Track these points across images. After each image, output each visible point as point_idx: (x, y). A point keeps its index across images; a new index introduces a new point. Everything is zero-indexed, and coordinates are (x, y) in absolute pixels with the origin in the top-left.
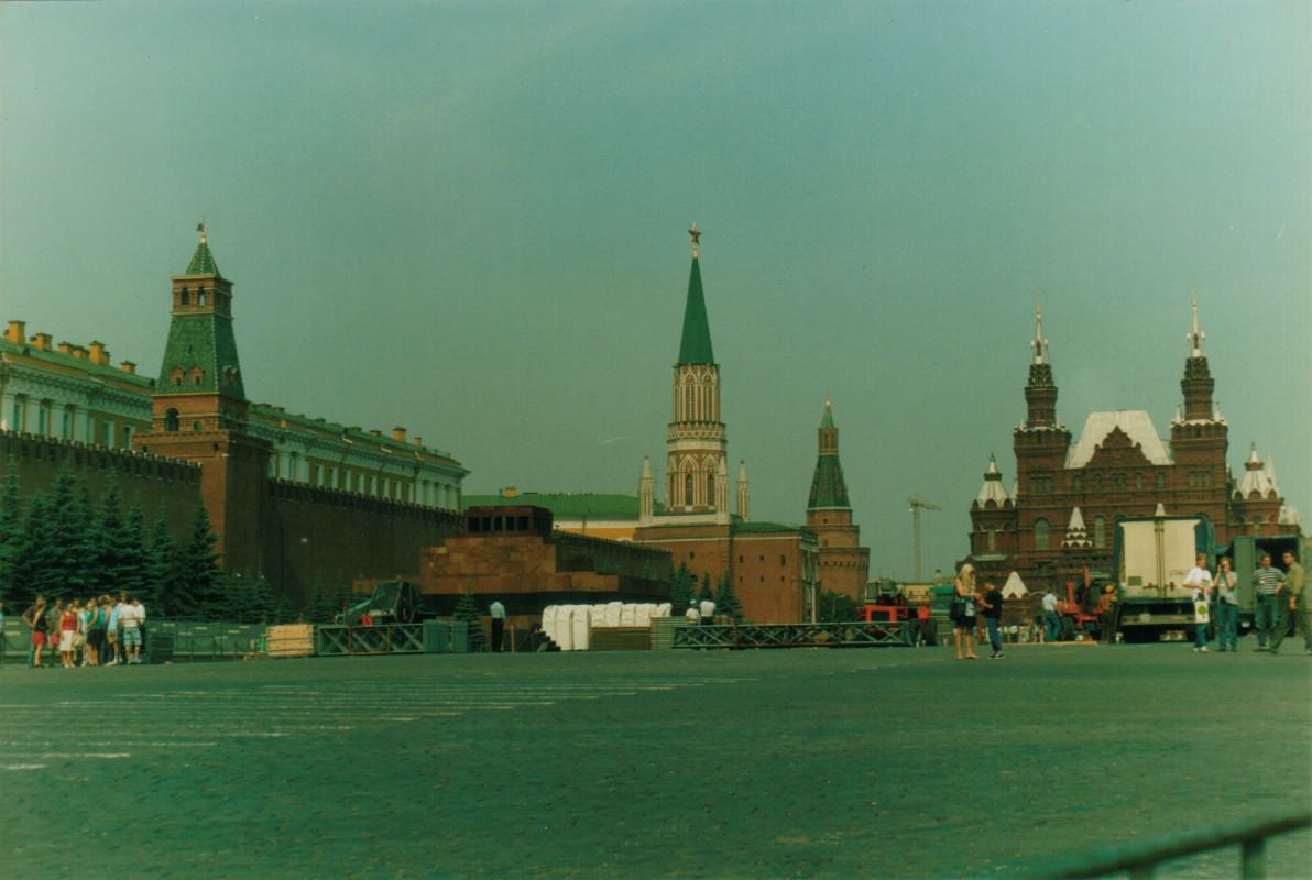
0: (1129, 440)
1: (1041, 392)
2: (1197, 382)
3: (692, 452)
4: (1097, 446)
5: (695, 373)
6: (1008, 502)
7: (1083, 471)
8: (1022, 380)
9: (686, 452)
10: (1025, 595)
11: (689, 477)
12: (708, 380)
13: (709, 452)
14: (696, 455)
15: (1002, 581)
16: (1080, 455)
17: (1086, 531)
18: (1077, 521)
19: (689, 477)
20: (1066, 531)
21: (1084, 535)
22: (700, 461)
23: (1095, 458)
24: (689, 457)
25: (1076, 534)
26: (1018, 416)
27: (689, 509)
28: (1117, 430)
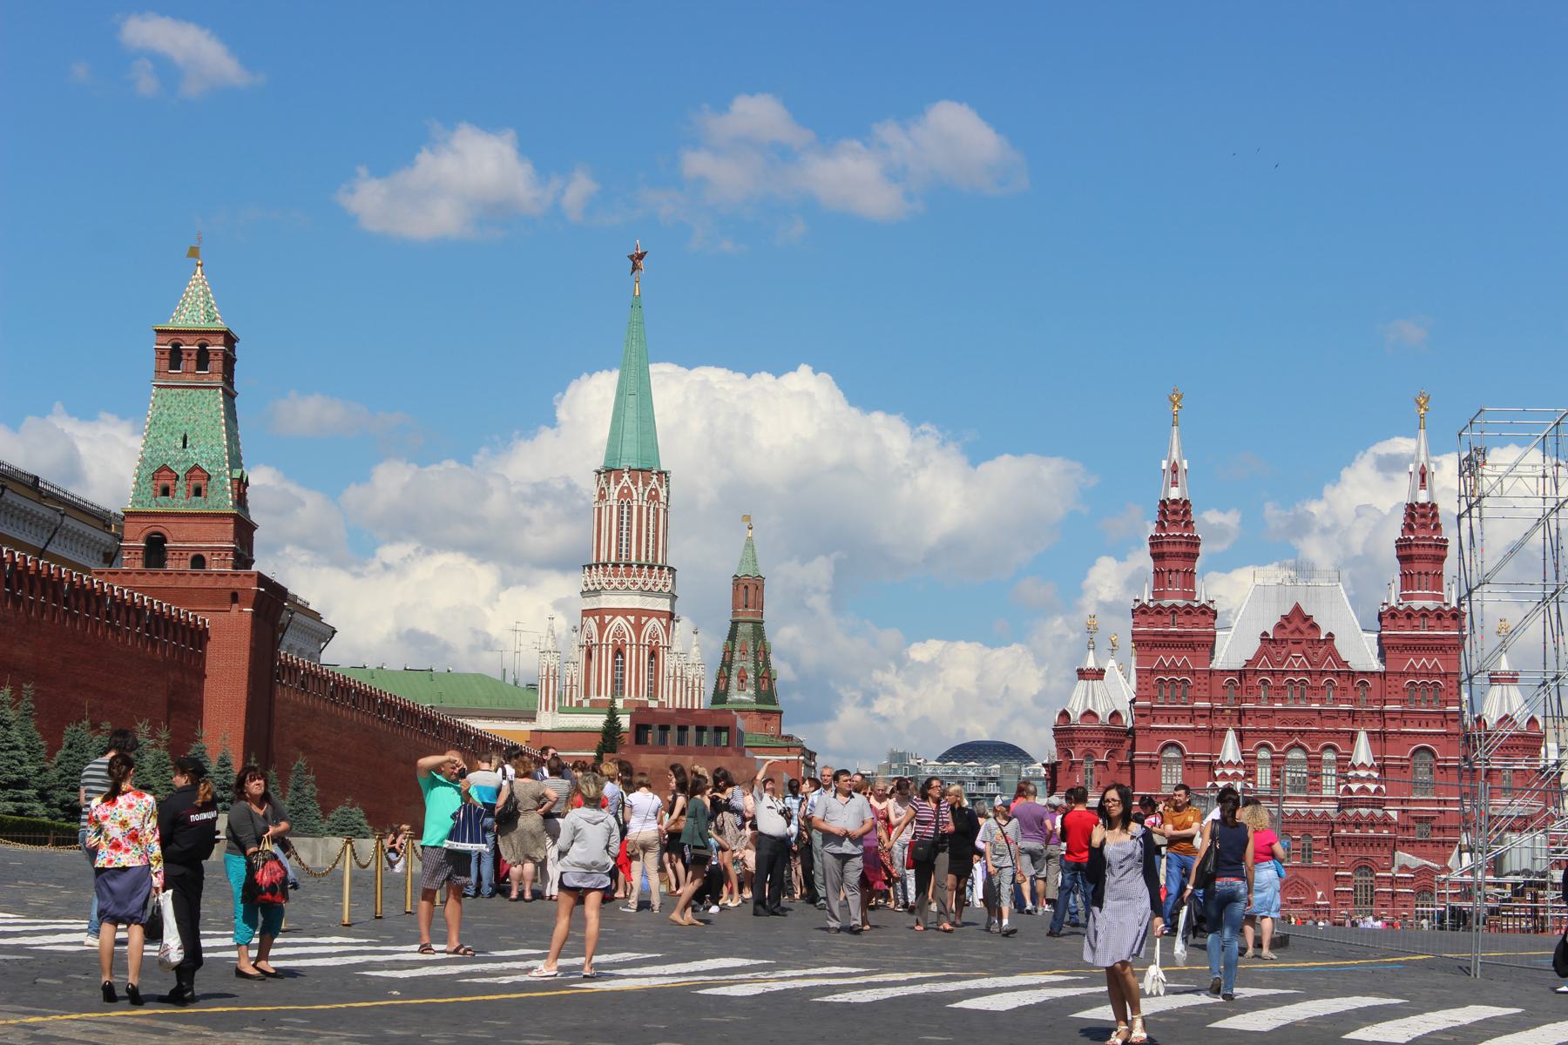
0: (1315, 627)
3: (624, 612)
4: (1265, 634)
5: (635, 483)
6: (1115, 715)
9: (615, 612)
11: (619, 652)
12: (654, 496)
13: (651, 614)
14: (632, 619)
16: (1233, 648)
18: (1230, 750)
19: (619, 652)
20: (1212, 767)
21: (1242, 772)
22: (638, 627)
24: (619, 620)
28: (1297, 609)
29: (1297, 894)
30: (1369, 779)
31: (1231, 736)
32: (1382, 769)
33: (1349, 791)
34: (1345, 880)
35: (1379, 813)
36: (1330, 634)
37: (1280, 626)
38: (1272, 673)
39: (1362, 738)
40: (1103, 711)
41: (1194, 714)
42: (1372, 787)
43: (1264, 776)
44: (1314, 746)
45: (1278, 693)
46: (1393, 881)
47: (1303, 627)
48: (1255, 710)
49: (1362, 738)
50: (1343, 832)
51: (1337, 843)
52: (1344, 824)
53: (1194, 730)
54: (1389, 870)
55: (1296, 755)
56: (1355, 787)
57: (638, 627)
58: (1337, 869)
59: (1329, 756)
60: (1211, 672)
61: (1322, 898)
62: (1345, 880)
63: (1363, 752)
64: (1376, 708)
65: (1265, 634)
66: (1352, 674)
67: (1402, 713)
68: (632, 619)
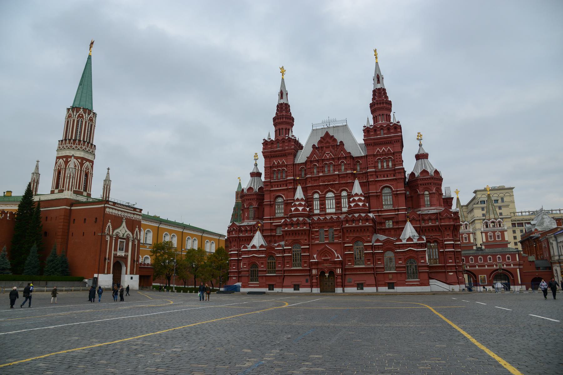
0: (335, 140)
1: (283, 117)
2: (380, 103)
4: (314, 145)
5: (73, 112)
7: (305, 164)
8: (273, 113)
10: (262, 246)
15: (251, 238)
17: (305, 201)
18: (299, 194)
23: (313, 153)
24: (61, 160)
25: (297, 203)
26: (270, 132)
27: (56, 191)
28: (327, 133)
29: (326, 256)
30: (360, 200)
31: (299, 189)
32: (368, 198)
33: (350, 206)
34: (350, 248)
35: (363, 215)
36: (341, 142)
37: (320, 142)
38: (318, 161)
39: (357, 183)
40: (256, 189)
41: (286, 183)
42: (361, 204)
43: (316, 204)
44: (337, 190)
45: (321, 169)
46: (372, 247)
47: (330, 141)
48: (311, 178)
49: (357, 183)
50: (347, 225)
51: (345, 231)
52: (347, 221)
53: (287, 189)
54: (370, 242)
55: (330, 195)
56: (352, 205)
57: (66, 163)
58: (345, 243)
59: (344, 193)
60: (294, 165)
61: (338, 257)
62: (350, 248)
63: (357, 189)
64: (364, 171)
65: (314, 145)
66: (352, 158)
67: (375, 172)
68: (64, 159)
